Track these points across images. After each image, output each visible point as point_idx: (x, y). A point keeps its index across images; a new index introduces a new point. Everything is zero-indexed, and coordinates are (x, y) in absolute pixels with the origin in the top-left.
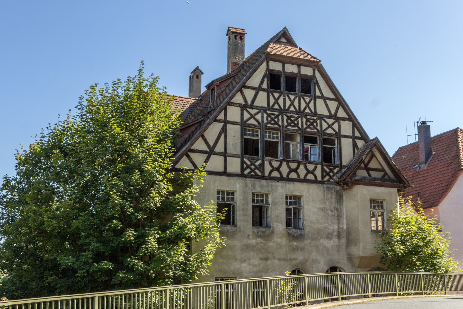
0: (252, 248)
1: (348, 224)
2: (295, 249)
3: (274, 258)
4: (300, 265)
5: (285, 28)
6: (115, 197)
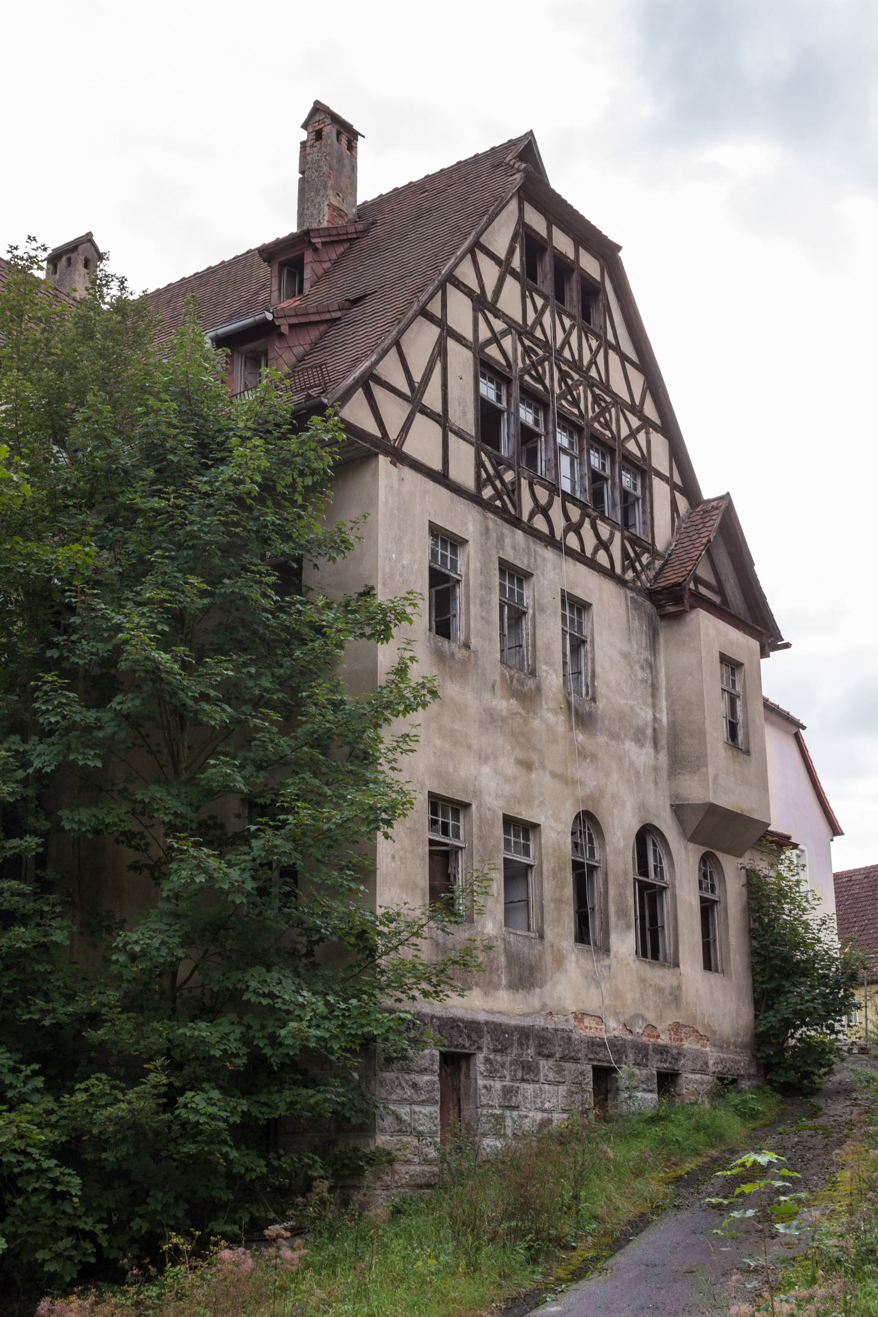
0: (500, 723)
1: (671, 712)
2: (583, 754)
3: (544, 768)
4: (590, 803)
5: (531, 133)
6: (103, 606)
